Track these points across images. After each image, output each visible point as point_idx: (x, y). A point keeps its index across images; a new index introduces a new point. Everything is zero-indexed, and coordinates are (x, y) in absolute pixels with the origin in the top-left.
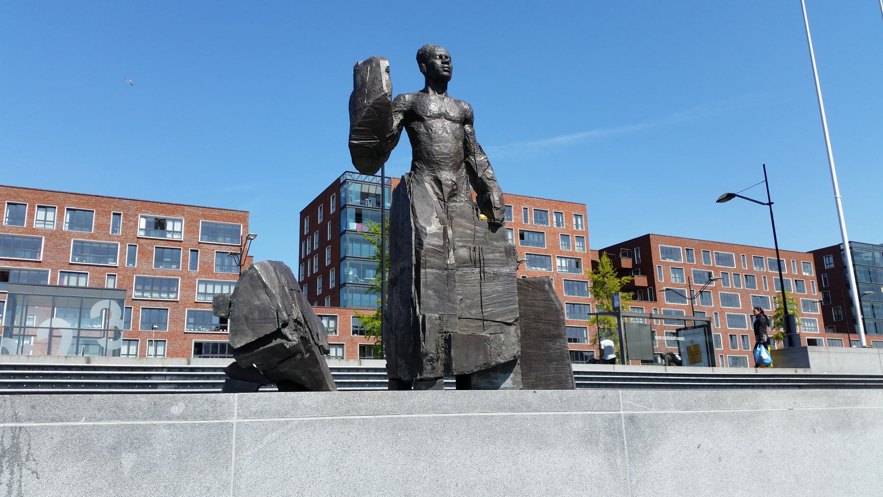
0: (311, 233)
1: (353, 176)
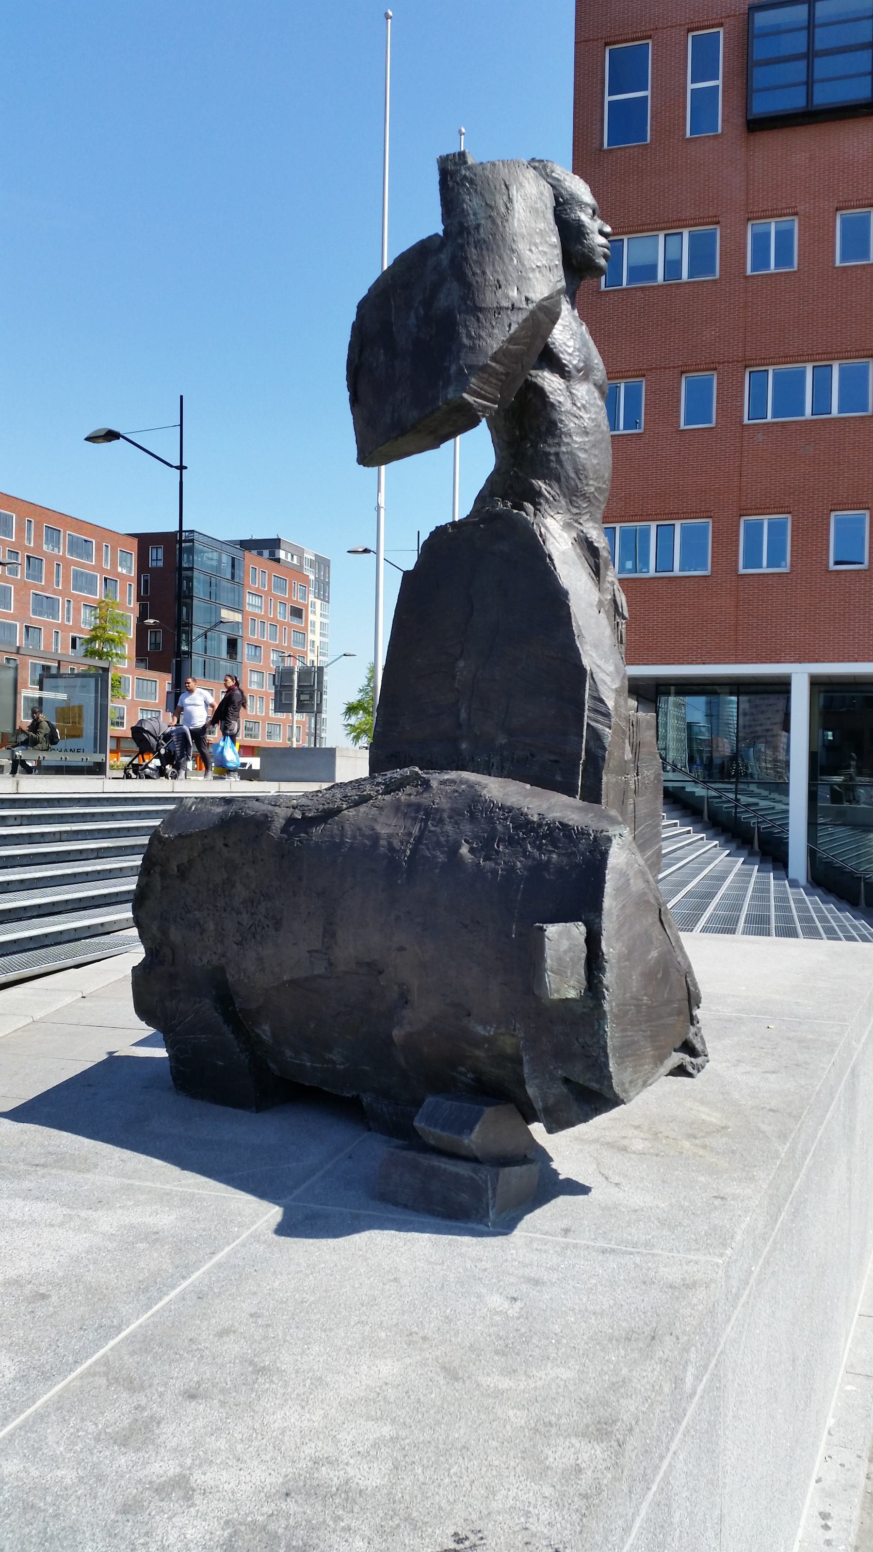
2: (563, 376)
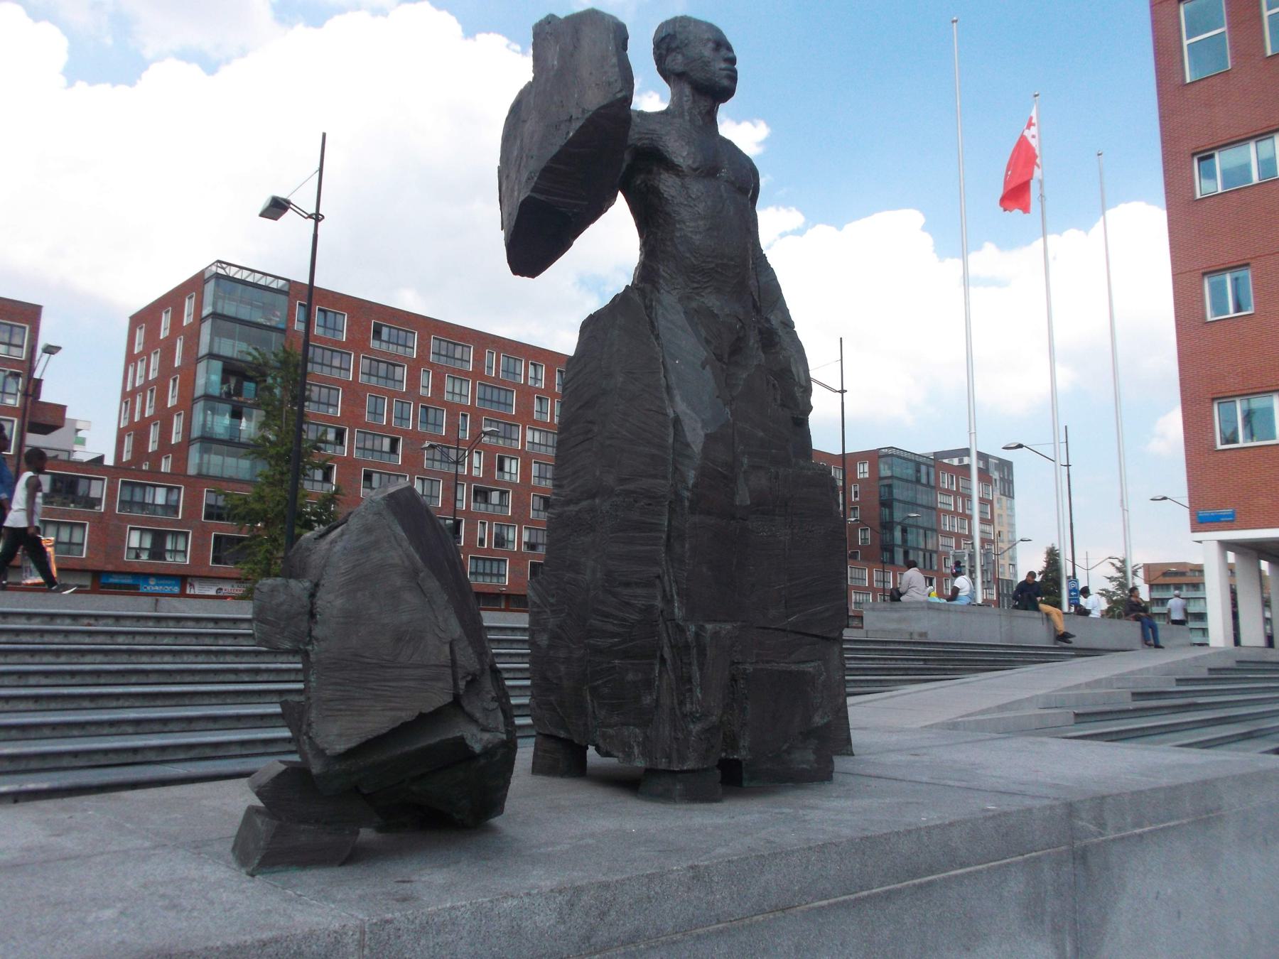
0: (146, 353)
1: (227, 270)
2: (678, 175)
